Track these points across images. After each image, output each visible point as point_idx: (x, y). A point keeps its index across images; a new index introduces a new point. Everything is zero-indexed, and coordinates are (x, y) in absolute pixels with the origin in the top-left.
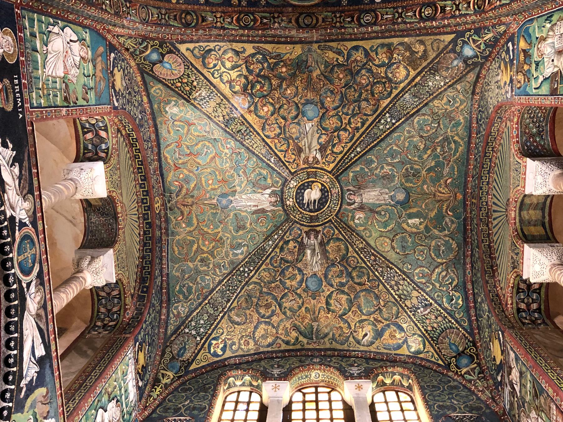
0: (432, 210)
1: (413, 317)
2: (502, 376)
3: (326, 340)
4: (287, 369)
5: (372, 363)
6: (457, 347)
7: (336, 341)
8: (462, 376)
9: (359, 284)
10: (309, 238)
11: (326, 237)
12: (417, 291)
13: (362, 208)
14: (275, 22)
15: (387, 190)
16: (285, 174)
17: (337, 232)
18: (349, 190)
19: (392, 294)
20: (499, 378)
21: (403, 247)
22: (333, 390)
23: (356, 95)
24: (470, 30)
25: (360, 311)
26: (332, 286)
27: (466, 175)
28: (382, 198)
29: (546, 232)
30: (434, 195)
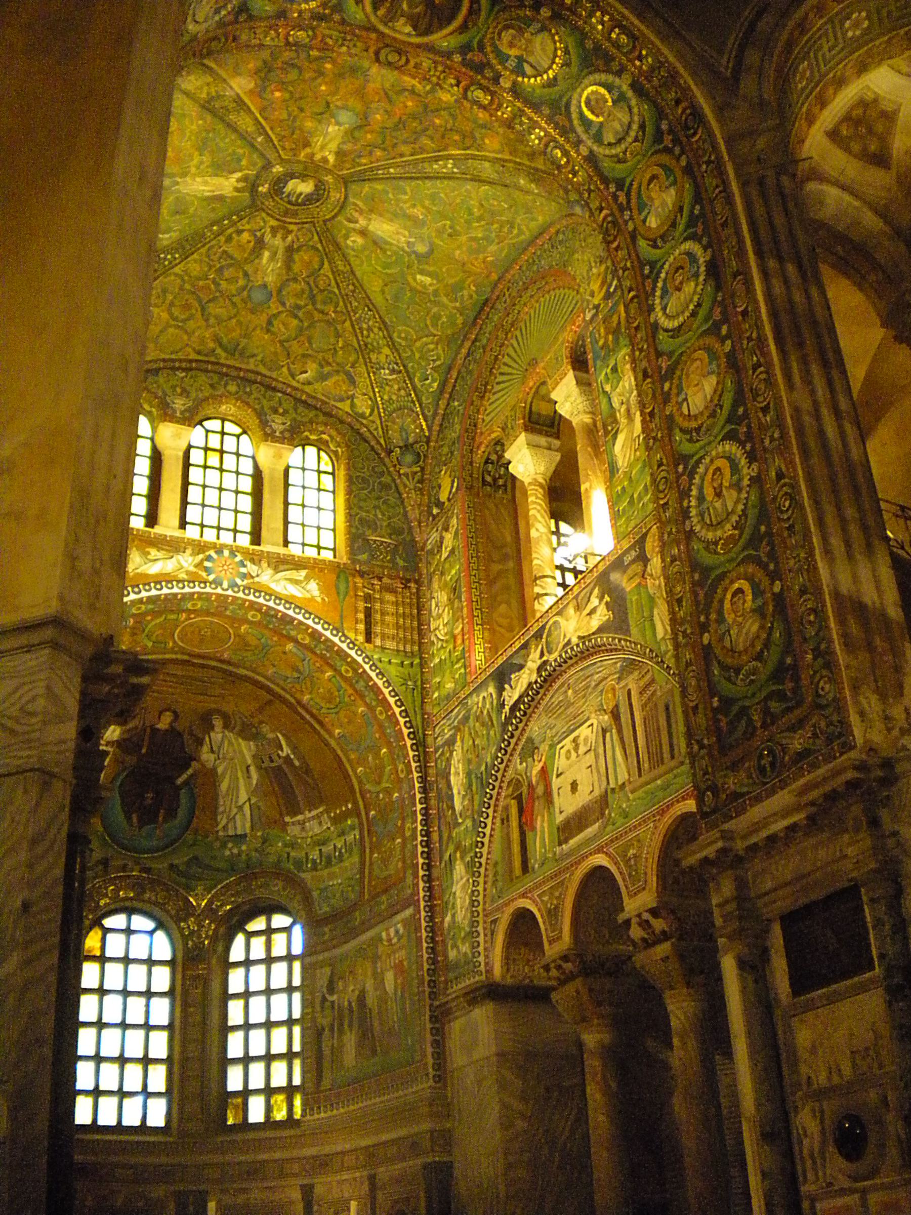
3: (252, 360)
4: (194, 400)
5: (301, 409)
7: (264, 365)
8: (400, 475)
9: (322, 312)
10: (274, 236)
13: (363, 233)
14: (343, 45)
15: (407, 233)
16: (272, 156)
17: (316, 238)
18: (356, 205)
22: (245, 432)
23: (419, 128)
25: (310, 343)
26: (284, 304)
27: (515, 261)
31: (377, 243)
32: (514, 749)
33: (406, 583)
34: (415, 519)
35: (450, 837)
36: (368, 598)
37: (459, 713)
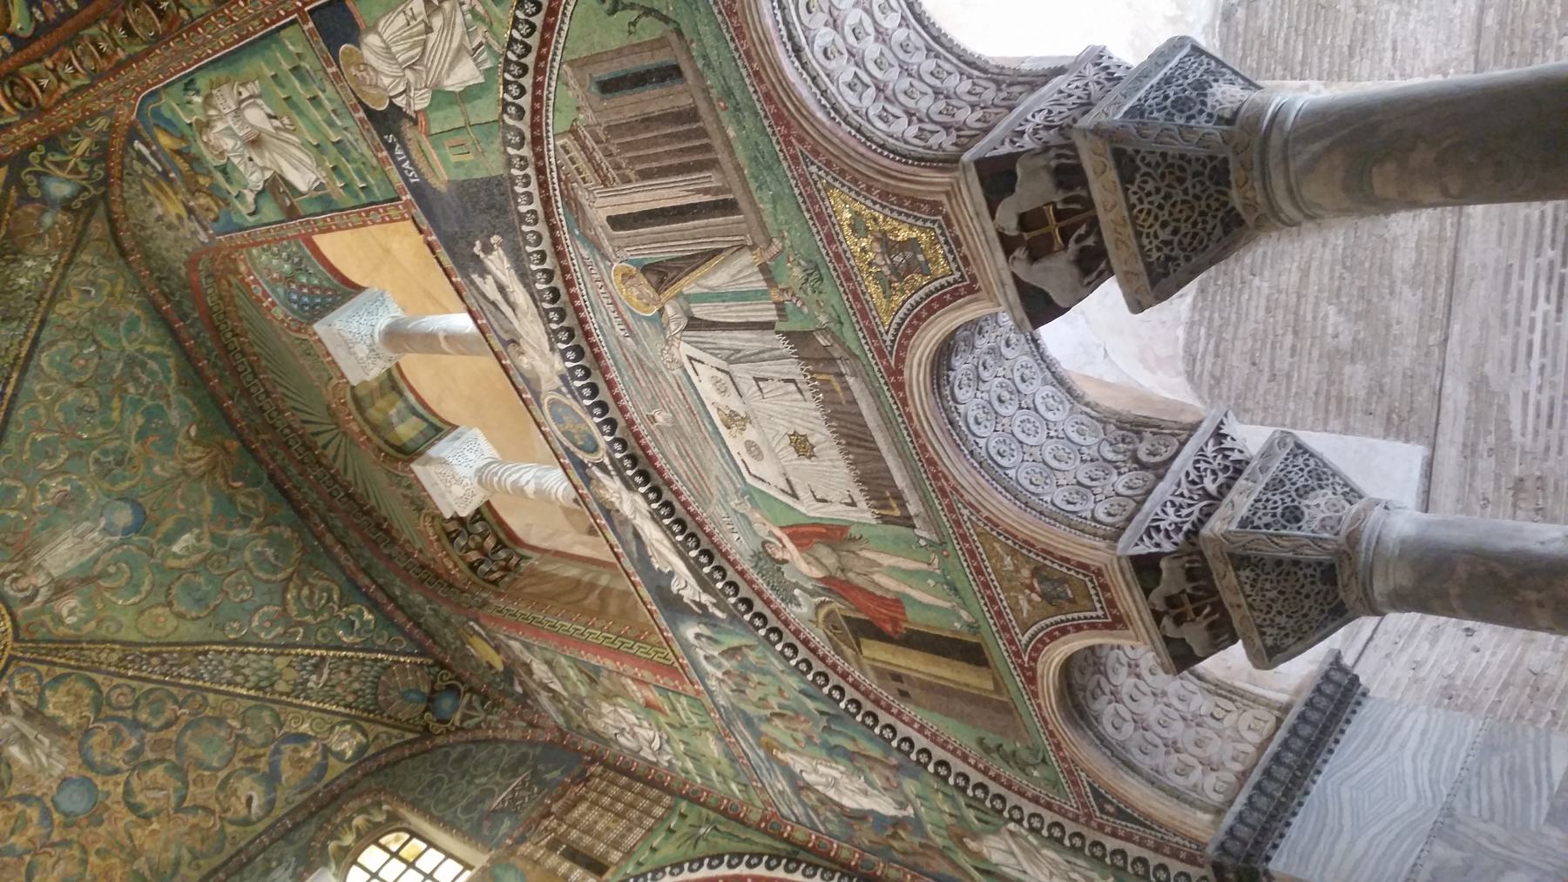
0: (202, 499)
1: (307, 703)
2: (521, 683)
3: (184, 870)
5: (296, 837)
6: (417, 691)
7: (204, 856)
9: (168, 725)
11: (27, 694)
12: (282, 654)
15: (86, 524)
17: (43, 668)
19: (241, 696)
20: (519, 689)
21: (198, 601)
24: (32, 147)
25: (208, 768)
26: (117, 771)
27: (216, 400)
28: (87, 545)
29: (426, 420)
30: (185, 472)
31: (86, 579)
32: (777, 612)
33: (584, 779)
34: (525, 730)
35: (942, 853)
36: (552, 847)
37: (745, 740)
